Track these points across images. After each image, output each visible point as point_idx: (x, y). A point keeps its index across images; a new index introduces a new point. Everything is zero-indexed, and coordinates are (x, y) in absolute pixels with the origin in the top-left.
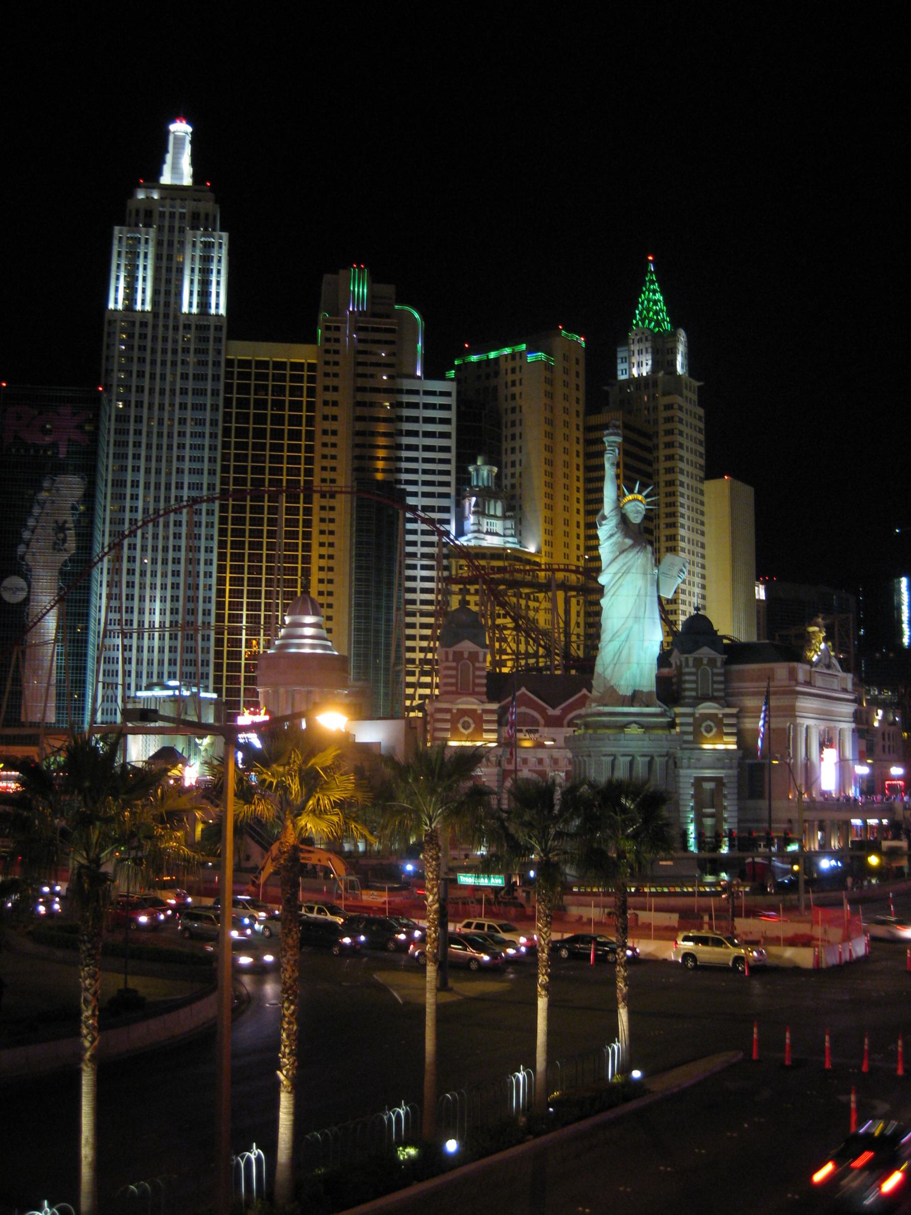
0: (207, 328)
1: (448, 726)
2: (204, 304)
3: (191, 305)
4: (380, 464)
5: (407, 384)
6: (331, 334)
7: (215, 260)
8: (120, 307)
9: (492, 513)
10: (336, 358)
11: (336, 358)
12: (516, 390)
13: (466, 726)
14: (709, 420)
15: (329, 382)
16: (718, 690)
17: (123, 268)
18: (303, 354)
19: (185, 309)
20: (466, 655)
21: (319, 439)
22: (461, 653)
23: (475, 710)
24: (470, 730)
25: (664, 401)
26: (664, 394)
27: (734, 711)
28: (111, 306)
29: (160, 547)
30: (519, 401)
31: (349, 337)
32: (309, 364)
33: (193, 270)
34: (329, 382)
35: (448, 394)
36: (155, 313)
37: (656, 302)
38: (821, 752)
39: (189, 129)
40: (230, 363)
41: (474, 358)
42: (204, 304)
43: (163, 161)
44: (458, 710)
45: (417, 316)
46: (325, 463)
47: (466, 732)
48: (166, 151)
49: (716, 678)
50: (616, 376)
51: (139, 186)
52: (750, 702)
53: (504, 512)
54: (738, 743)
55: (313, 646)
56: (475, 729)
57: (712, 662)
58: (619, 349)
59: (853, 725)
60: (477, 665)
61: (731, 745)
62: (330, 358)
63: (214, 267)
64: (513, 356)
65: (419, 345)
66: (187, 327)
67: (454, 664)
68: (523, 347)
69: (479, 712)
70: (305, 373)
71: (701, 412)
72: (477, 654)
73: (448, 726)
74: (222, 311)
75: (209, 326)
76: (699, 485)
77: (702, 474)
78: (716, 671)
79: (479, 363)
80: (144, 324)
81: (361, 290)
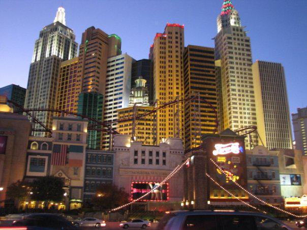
9: (139, 96)
36: (40, 61)
42: (50, 54)
76: (246, 67)
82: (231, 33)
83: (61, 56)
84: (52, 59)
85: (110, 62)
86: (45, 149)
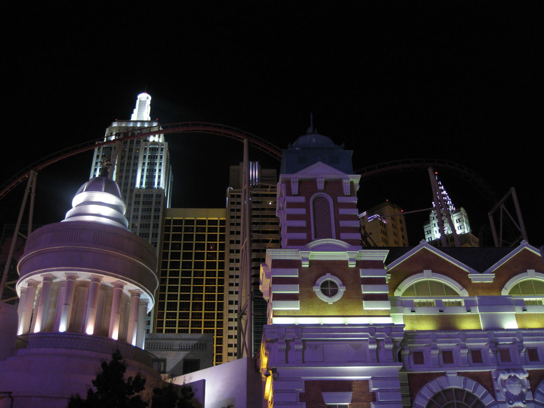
0: (152, 196)
1: (295, 290)
3: (141, 183)
6: (234, 200)
7: (159, 157)
13: (329, 290)
15: (233, 229)
17: (99, 164)
18: (216, 215)
19: (138, 185)
20: (321, 186)
21: (227, 265)
22: (313, 182)
23: (345, 263)
24: (337, 298)
32: (221, 221)
33: (144, 164)
34: (233, 229)
39: (150, 98)
43: (132, 113)
44: (312, 262)
46: (232, 281)
47: (330, 301)
48: (135, 108)
51: (115, 121)
56: (346, 296)
58: (425, 227)
60: (340, 199)
62: (233, 214)
63: (158, 162)
66: (138, 196)
67: (302, 199)
69: (352, 265)
70: (218, 226)
72: (339, 183)
73: (295, 290)
74: (162, 186)
75: (152, 195)
81: (254, 173)
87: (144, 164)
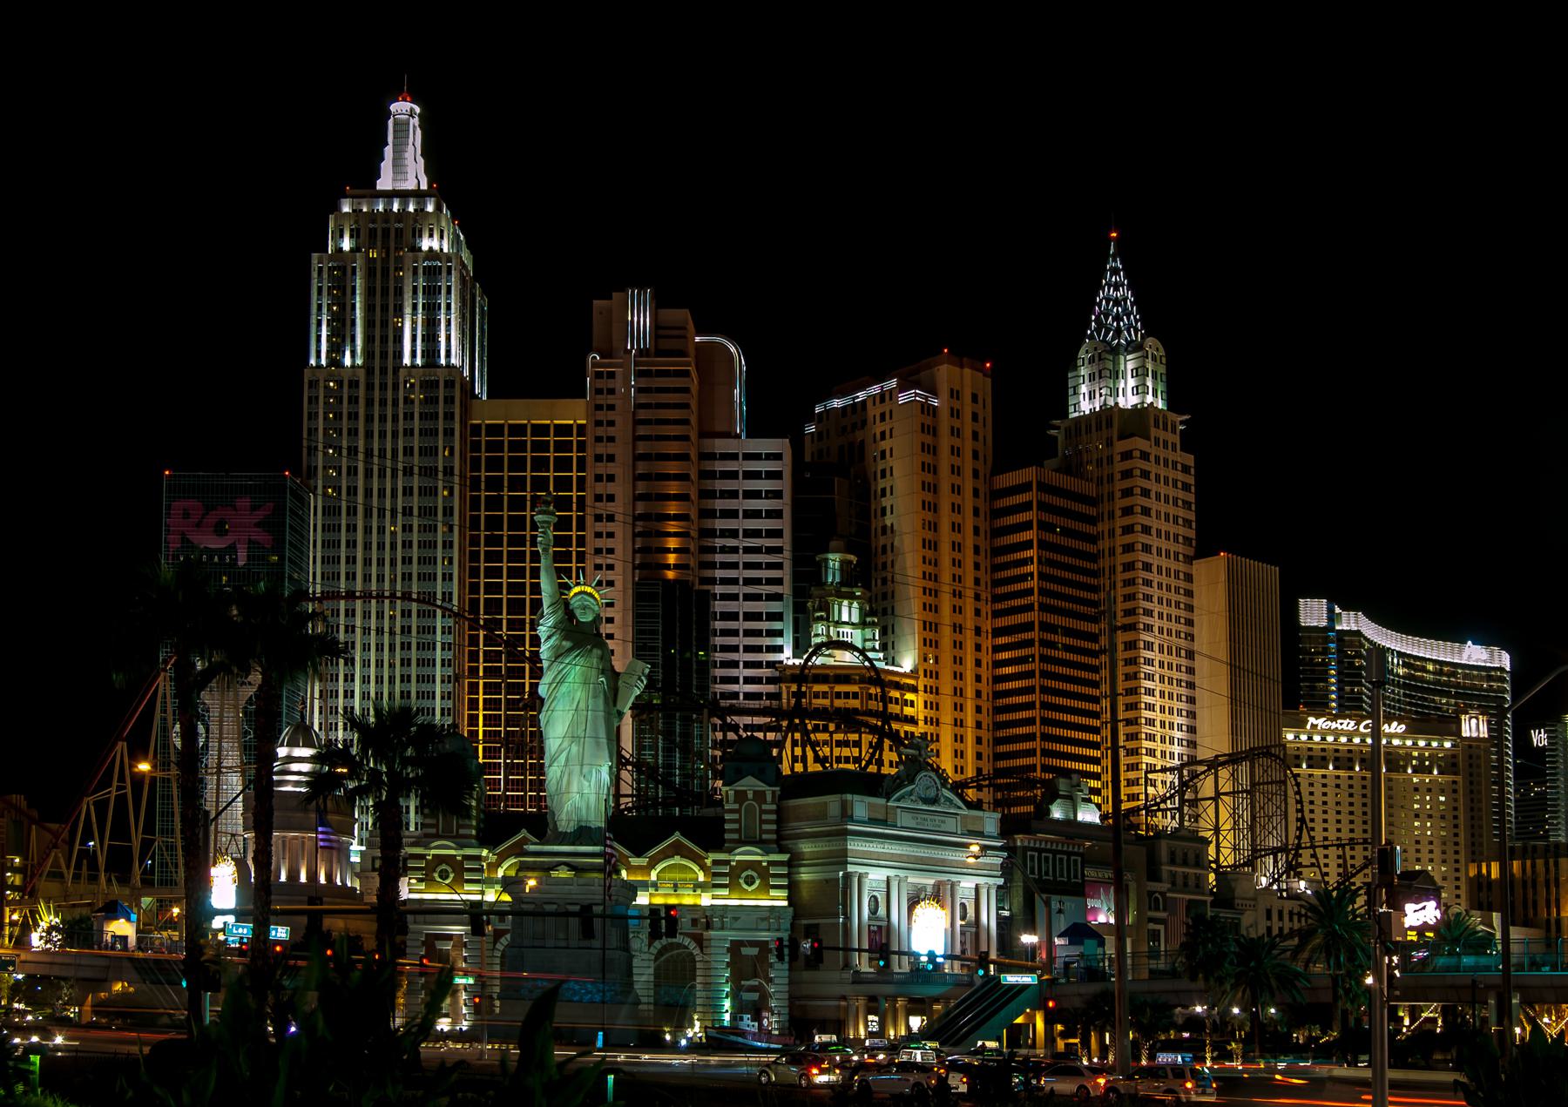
2: (431, 352)
4: (672, 559)
5: (721, 446)
8: (324, 362)
10: (611, 415)
11: (611, 415)
12: (885, 445)
14: (1201, 471)
15: (601, 449)
16: (768, 832)
17: (325, 310)
19: (407, 361)
25: (1120, 446)
26: (1123, 436)
27: (785, 857)
28: (313, 362)
29: (373, 678)
30: (890, 462)
31: (629, 387)
33: (415, 307)
34: (601, 449)
35: (777, 457)
36: (368, 367)
37: (1117, 303)
38: (911, 909)
40: (476, 429)
41: (837, 403)
42: (431, 352)
45: (733, 349)
49: (765, 817)
50: (1067, 413)
52: (806, 847)
53: (863, 614)
54: (789, 898)
55: (297, 784)
57: (759, 796)
59: (1001, 881)
61: (777, 899)
62: (601, 416)
64: (882, 396)
65: (737, 391)
68: (893, 383)
71: (1190, 460)
76: (1182, 567)
77: (1191, 552)
78: (764, 807)
79: (844, 408)
80: (354, 384)
82: (1148, 439)
83: (466, 373)
84: (449, 384)
85: (712, 456)
86: (1157, 909)
87: (415, 307)
